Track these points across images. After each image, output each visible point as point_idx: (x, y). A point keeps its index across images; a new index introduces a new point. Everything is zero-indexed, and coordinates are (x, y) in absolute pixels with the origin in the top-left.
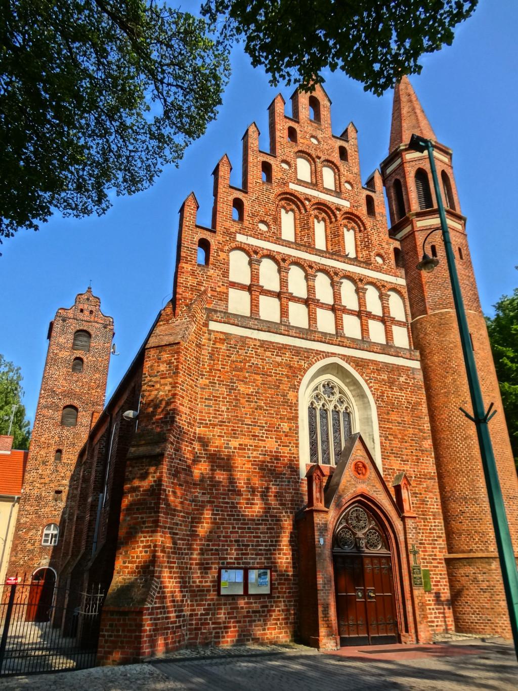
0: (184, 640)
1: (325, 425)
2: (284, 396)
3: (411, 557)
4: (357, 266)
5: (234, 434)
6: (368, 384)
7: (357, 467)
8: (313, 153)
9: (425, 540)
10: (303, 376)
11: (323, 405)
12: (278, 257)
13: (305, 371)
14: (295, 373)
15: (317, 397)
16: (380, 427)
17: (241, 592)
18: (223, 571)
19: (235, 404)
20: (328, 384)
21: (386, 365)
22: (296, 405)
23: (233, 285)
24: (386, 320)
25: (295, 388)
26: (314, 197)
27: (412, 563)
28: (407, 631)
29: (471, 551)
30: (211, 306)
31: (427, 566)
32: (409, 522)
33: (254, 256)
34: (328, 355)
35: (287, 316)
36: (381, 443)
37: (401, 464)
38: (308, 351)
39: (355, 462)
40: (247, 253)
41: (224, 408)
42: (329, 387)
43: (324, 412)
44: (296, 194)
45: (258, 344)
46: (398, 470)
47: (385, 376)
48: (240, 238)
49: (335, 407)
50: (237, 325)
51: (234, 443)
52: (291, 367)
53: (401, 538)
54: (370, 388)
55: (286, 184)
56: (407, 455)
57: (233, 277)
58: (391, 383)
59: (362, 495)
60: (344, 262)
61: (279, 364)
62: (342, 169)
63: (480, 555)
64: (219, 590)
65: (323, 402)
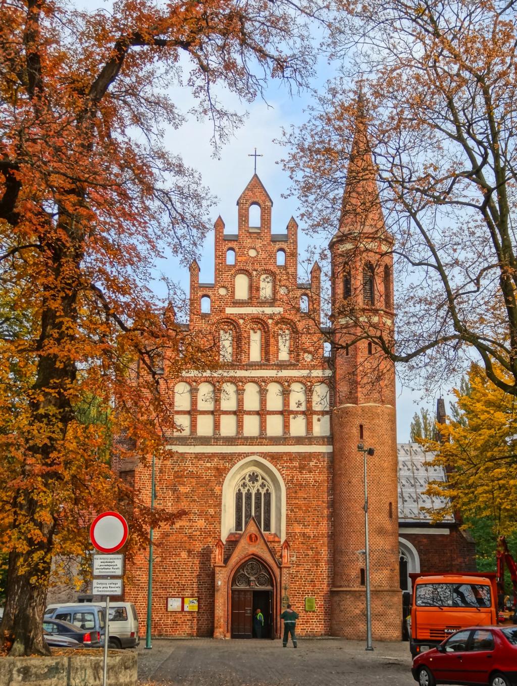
1: (249, 505)
2: (212, 490)
3: (283, 591)
6: (280, 472)
7: (250, 537)
8: (249, 268)
11: (248, 490)
13: (229, 470)
14: (221, 473)
15: (244, 485)
16: (287, 503)
17: (180, 610)
19: (178, 499)
20: (253, 474)
22: (221, 495)
23: (178, 412)
25: (221, 484)
26: (248, 315)
27: (283, 595)
29: (341, 586)
32: (285, 570)
35: (219, 429)
39: (248, 535)
40: (189, 384)
41: (170, 504)
42: (254, 478)
43: (249, 496)
44: (232, 317)
47: (296, 464)
49: (258, 490)
52: (218, 469)
53: (279, 580)
54: (282, 475)
55: (222, 311)
58: (302, 468)
59: (253, 554)
61: (209, 468)
64: (167, 609)
65: (248, 488)
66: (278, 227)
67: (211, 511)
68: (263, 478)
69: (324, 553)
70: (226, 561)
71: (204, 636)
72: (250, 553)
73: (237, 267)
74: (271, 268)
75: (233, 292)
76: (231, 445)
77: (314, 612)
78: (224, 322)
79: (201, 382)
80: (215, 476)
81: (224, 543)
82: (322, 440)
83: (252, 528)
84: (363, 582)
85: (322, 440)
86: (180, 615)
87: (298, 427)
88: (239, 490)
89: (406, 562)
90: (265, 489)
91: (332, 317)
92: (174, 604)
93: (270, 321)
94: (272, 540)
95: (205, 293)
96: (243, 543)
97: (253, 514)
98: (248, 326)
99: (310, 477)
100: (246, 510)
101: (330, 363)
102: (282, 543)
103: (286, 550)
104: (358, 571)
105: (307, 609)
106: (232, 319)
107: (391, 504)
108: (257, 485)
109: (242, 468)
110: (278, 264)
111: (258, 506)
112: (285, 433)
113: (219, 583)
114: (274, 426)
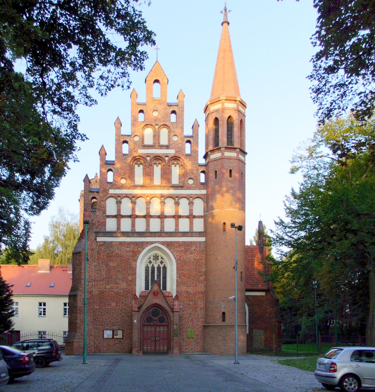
2: (130, 265)
3: (175, 326)
5: (108, 283)
6: (173, 254)
8: (154, 124)
10: (139, 255)
11: (153, 265)
12: (131, 197)
13: (141, 252)
14: (135, 254)
15: (150, 262)
16: (177, 273)
17: (111, 337)
20: (156, 255)
21: (185, 242)
22: (136, 268)
23: (108, 216)
24: (191, 217)
25: (136, 261)
26: (152, 154)
28: (170, 350)
29: (210, 323)
30: (98, 230)
33: (119, 199)
34: (152, 243)
38: (142, 243)
40: (115, 198)
41: (104, 274)
42: (156, 257)
43: (153, 268)
44: (142, 155)
45: (119, 244)
48: (112, 191)
50: (109, 237)
51: (108, 287)
52: (134, 252)
53: (172, 319)
57: (108, 213)
58: (186, 251)
59: (156, 304)
61: (128, 251)
62: (171, 128)
63: (212, 324)
66: (172, 99)
67: (130, 278)
68: (162, 258)
69: (201, 304)
70: (139, 308)
71: (126, 353)
72: (154, 302)
73: (145, 123)
74: (167, 123)
75: (143, 139)
76: (142, 237)
77: (193, 338)
79: (123, 197)
80: (132, 256)
81: (138, 297)
82: (200, 234)
83: (156, 288)
84: (224, 320)
85: (200, 234)
86: (111, 340)
87: (184, 225)
88: (147, 265)
90: (163, 265)
91: (205, 157)
92: (108, 334)
93: (167, 159)
94: (167, 295)
95: (124, 139)
96: (150, 296)
97: (156, 279)
98: (153, 162)
99: (191, 256)
100: (151, 278)
101: (205, 185)
102: (174, 297)
103: (176, 301)
104: (221, 314)
105: (189, 337)
107: (241, 272)
108: (158, 262)
109: (149, 251)
110: (171, 122)
111: (159, 276)
112: (176, 229)
113: (135, 321)
114: (169, 225)
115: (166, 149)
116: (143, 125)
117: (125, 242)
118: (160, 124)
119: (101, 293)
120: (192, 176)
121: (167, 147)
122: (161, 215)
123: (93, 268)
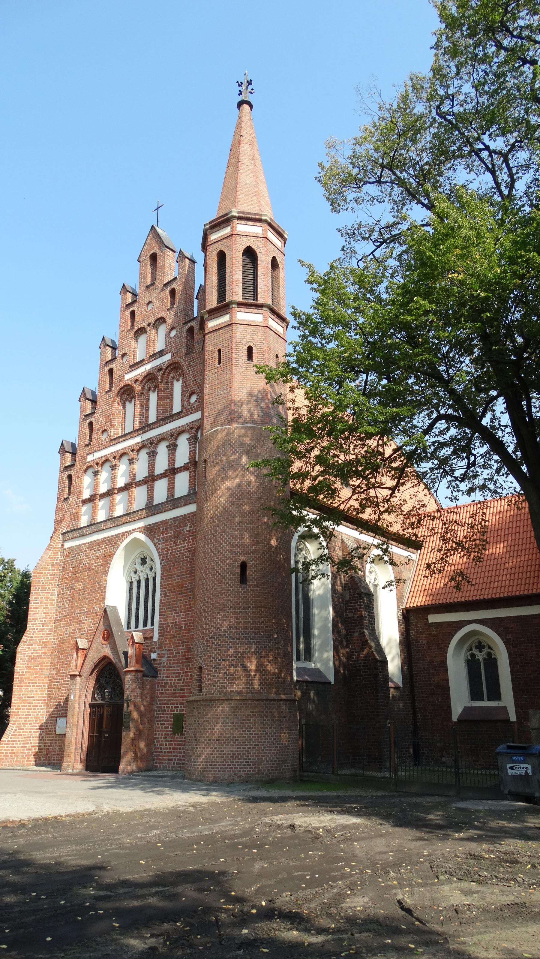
0: (40, 760)
4: (170, 422)
9: (186, 686)
10: (111, 561)
12: (111, 458)
13: (114, 555)
15: (136, 572)
18: (58, 719)
21: (174, 519)
22: (105, 587)
23: (84, 502)
25: (106, 573)
31: (183, 710)
34: (129, 533)
36: (161, 600)
37: (174, 616)
43: (139, 582)
44: (129, 383)
46: (171, 623)
48: (90, 458)
51: (70, 630)
54: (157, 550)
56: (181, 606)
60: (160, 426)
74: (163, 314)
78: (125, 391)
89: (495, 660)
95: (110, 366)
98: (146, 387)
106: (129, 385)
115: (160, 357)
116: (133, 332)
117: (95, 541)
118: (152, 321)
119: (61, 643)
120: (195, 388)
121: (161, 353)
122: (149, 476)
123: (55, 597)
